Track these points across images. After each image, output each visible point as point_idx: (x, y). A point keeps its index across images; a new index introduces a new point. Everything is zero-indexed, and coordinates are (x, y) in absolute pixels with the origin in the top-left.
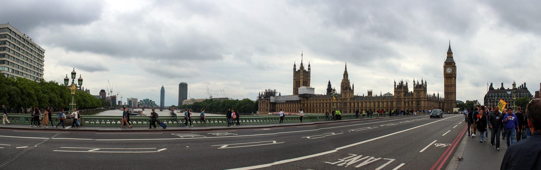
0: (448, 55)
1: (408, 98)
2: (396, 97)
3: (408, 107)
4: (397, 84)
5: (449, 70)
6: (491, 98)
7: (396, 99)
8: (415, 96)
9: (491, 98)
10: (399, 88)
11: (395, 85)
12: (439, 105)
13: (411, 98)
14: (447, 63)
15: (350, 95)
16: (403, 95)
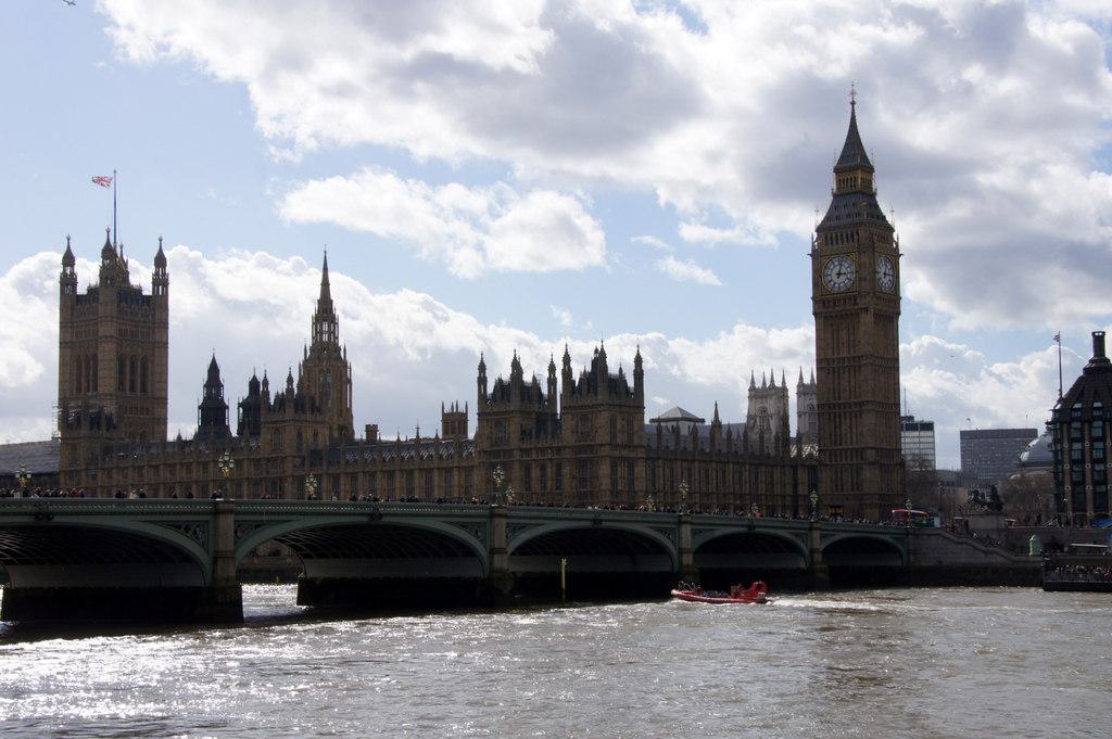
0: (839, 182)
1: (542, 450)
2: (486, 445)
3: (543, 495)
4: (501, 371)
5: (841, 275)
6: (1082, 430)
7: (485, 452)
8: (568, 436)
9: (1082, 430)
10: (499, 395)
11: (482, 381)
12: (788, 479)
13: (551, 448)
14: (830, 228)
15: (300, 435)
16: (518, 434)
